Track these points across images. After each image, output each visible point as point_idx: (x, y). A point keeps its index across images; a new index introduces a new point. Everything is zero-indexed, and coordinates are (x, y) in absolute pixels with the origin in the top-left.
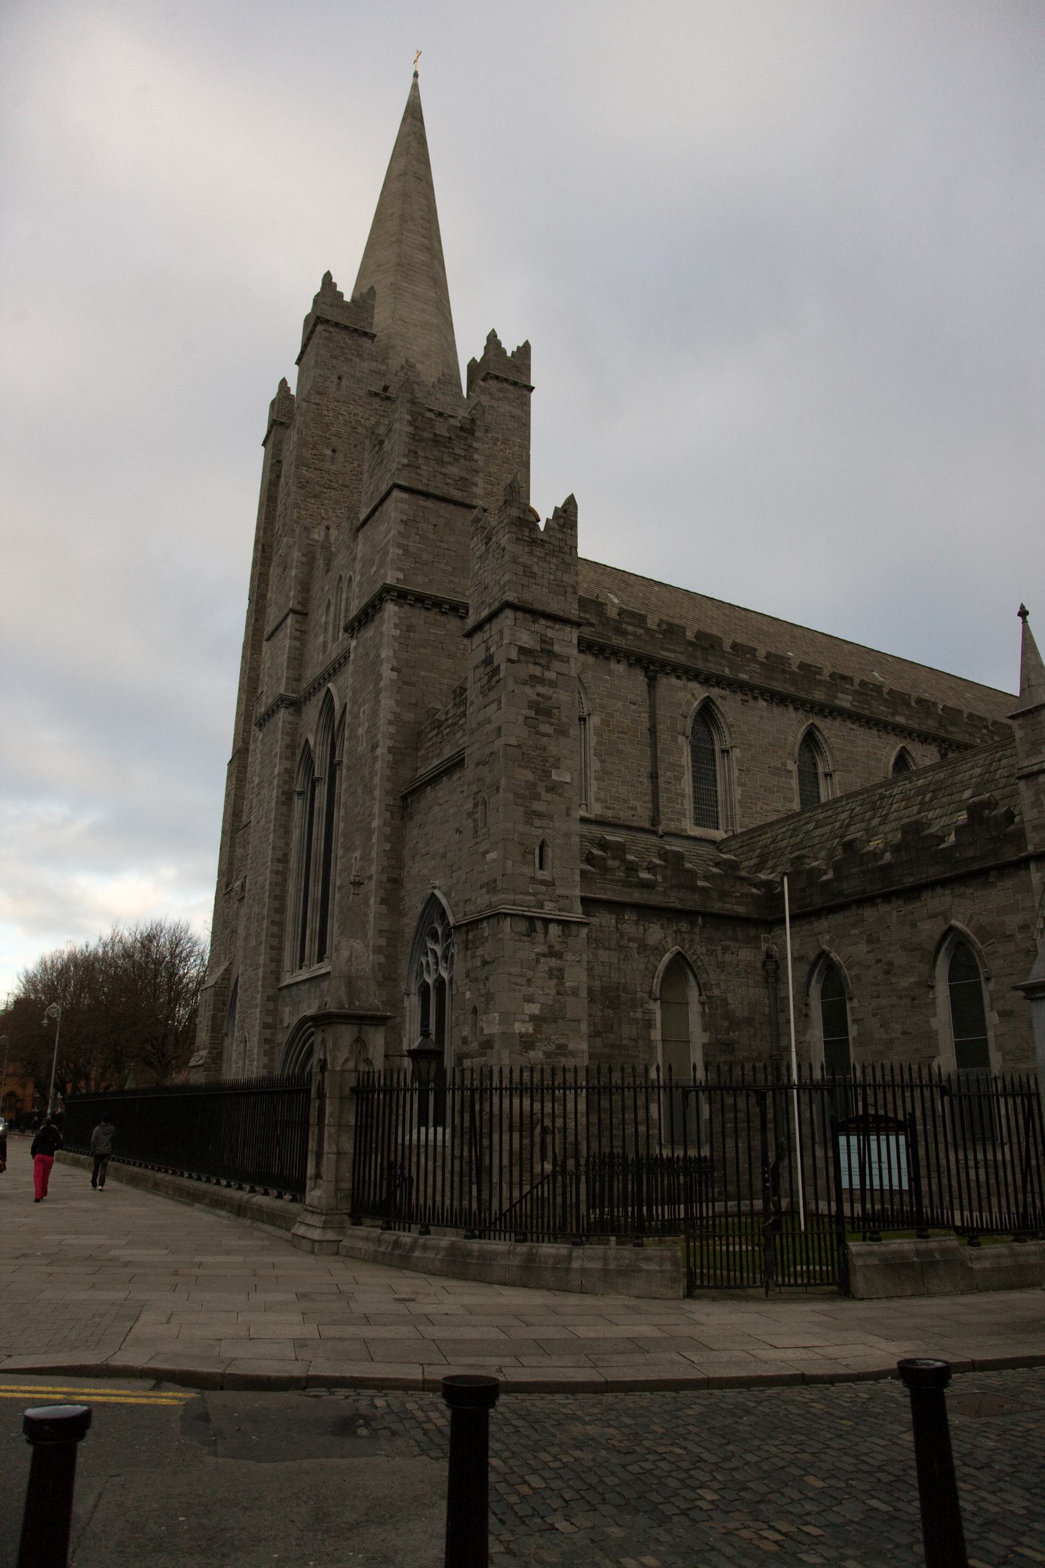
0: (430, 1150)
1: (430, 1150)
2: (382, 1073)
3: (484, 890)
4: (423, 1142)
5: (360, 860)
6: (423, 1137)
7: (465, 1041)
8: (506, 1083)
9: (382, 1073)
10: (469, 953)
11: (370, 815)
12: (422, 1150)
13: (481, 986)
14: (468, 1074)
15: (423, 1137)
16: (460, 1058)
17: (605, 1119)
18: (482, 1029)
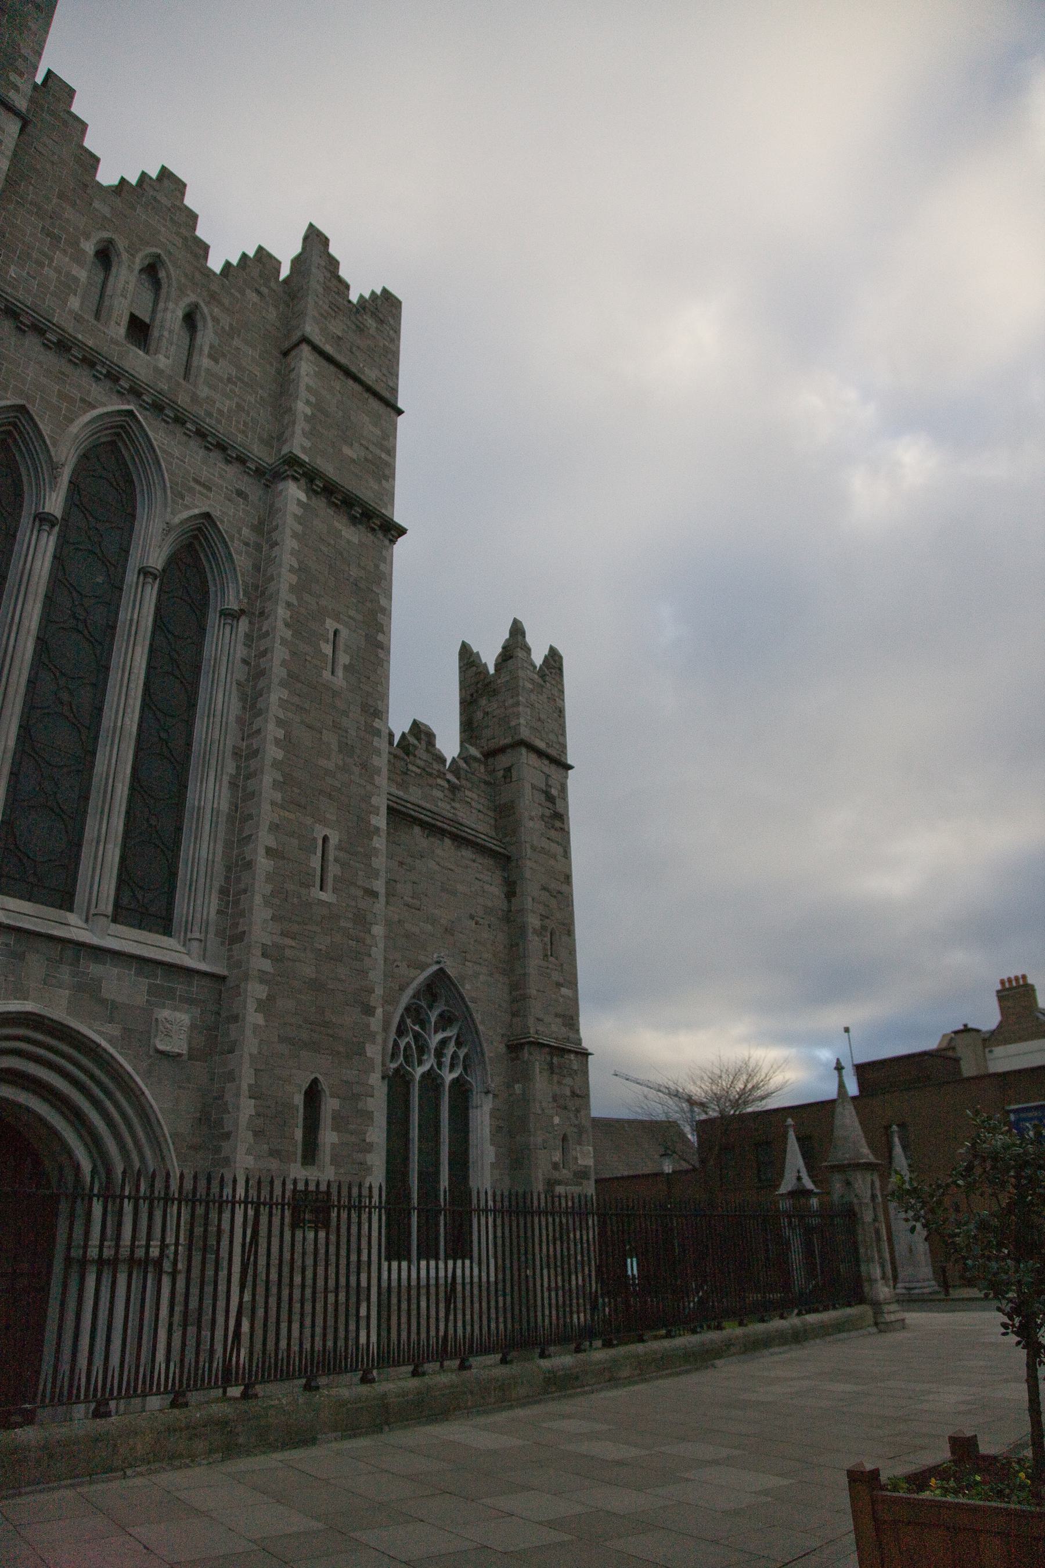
0: (433, 1290)
1: (433, 1290)
2: (490, 1193)
3: (559, 1020)
4: (423, 1282)
5: (339, 848)
6: (394, 1276)
7: (555, 1166)
8: (344, 1200)
9: (490, 1193)
10: (555, 1078)
11: (367, 798)
12: (423, 1291)
13: (572, 1115)
14: (557, 1199)
15: (394, 1276)
16: (551, 1184)
17: (155, 1247)
18: (576, 1158)
